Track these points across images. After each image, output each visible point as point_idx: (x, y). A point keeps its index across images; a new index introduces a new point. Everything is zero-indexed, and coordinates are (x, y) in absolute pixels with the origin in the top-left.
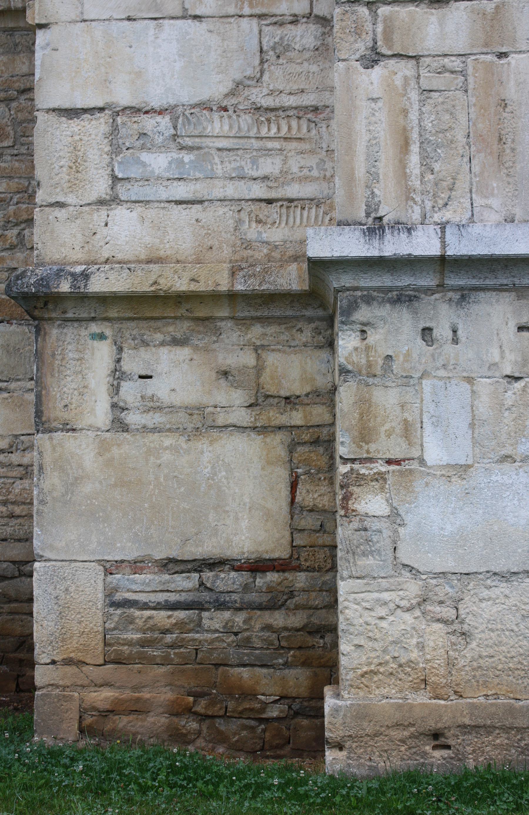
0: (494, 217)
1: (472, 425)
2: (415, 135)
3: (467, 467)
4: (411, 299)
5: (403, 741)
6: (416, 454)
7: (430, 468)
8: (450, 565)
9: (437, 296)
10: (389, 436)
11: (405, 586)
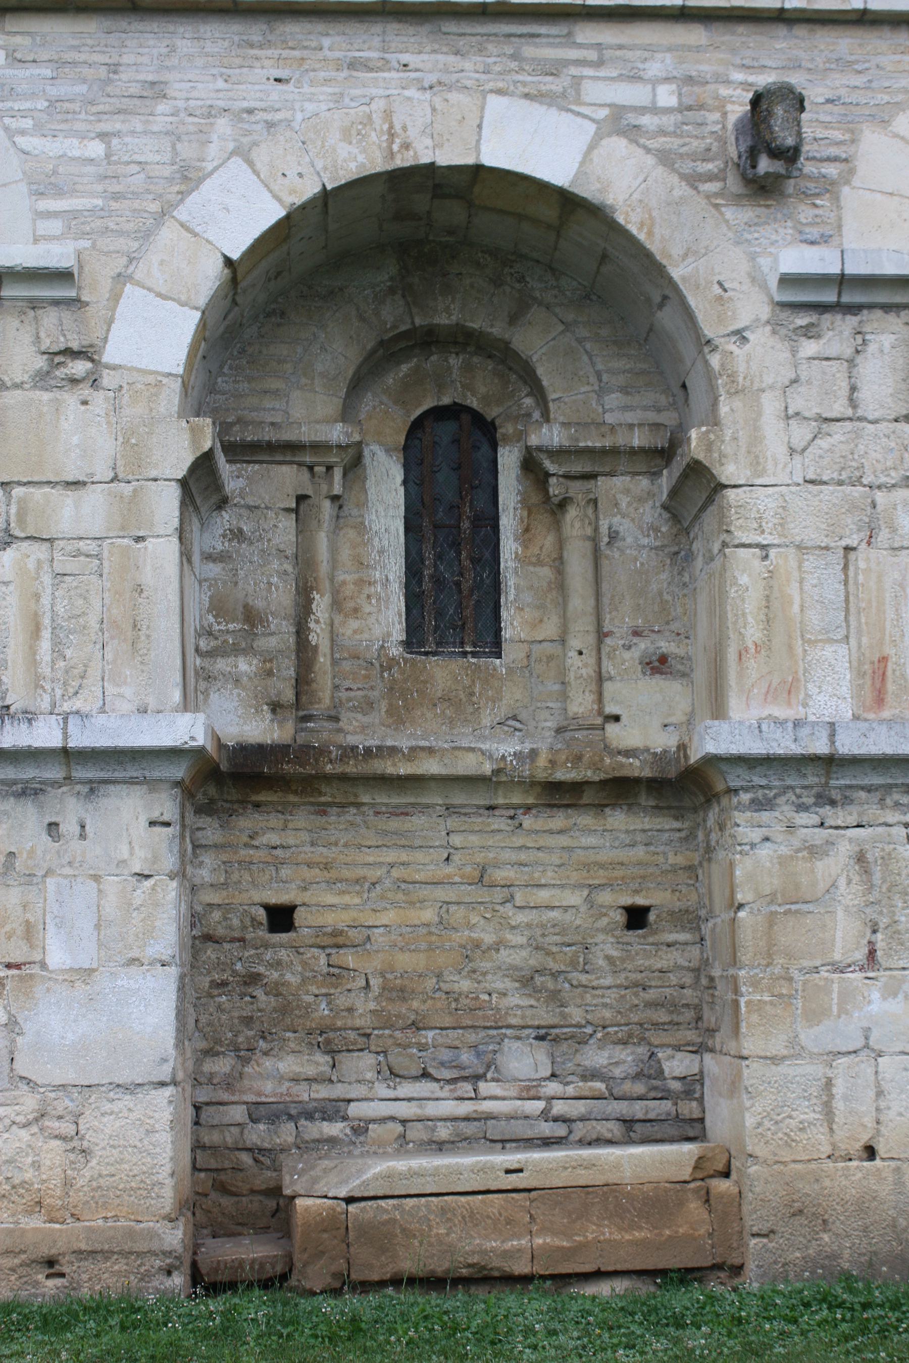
0: (126, 707)
1: (98, 927)
2: (47, 621)
3: (91, 971)
4: (36, 792)
5: (13, 1270)
6: (37, 957)
7: (51, 972)
8: (70, 1076)
9: (64, 789)
10: (9, 938)
11: (21, 1101)
